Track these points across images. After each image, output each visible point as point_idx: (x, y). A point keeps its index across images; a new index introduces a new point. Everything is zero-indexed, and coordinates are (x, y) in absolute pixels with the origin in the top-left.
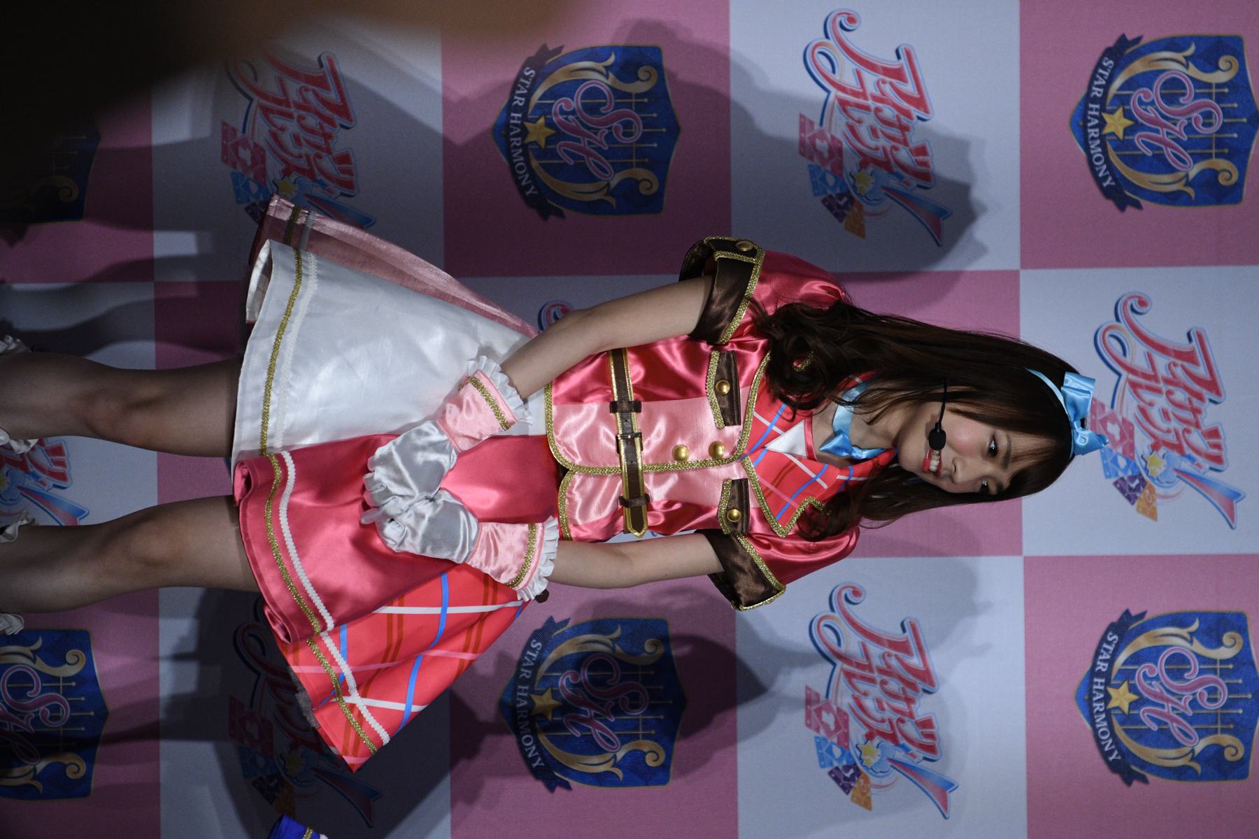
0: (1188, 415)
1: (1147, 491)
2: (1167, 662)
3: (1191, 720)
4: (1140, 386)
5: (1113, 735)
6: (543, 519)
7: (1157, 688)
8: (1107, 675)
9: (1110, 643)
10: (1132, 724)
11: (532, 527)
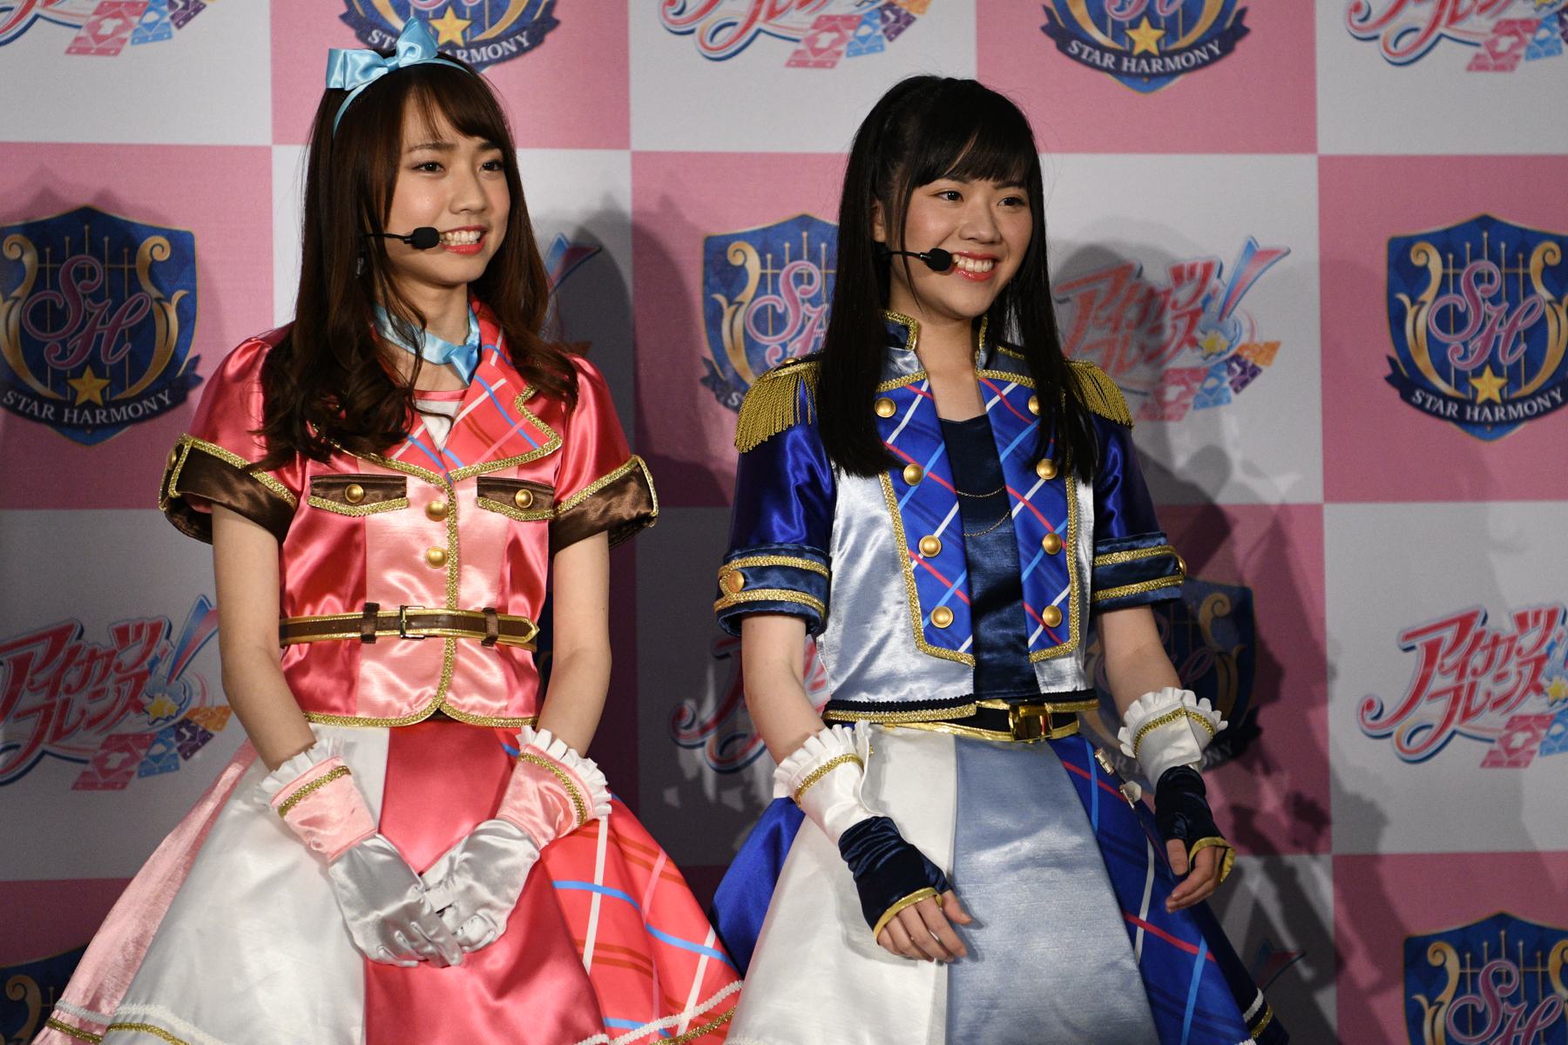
5: (498, 40)
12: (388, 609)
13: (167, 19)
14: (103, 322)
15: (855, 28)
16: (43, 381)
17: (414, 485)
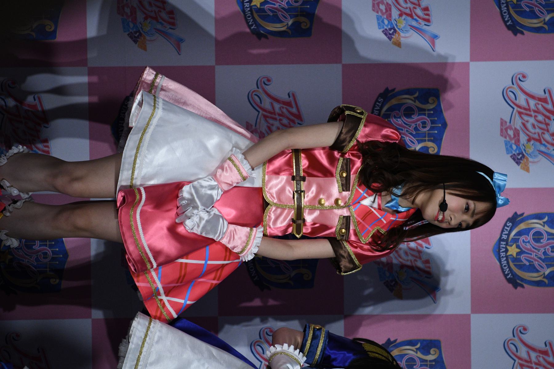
0: (544, 126)
1: (525, 160)
2: (533, 235)
3: (543, 261)
5: (509, 267)
6: (256, 226)
7: (528, 246)
8: (507, 241)
9: (508, 227)
10: (517, 262)
11: (251, 230)
13: (514, 152)
14: (407, 131)
16: (387, 111)
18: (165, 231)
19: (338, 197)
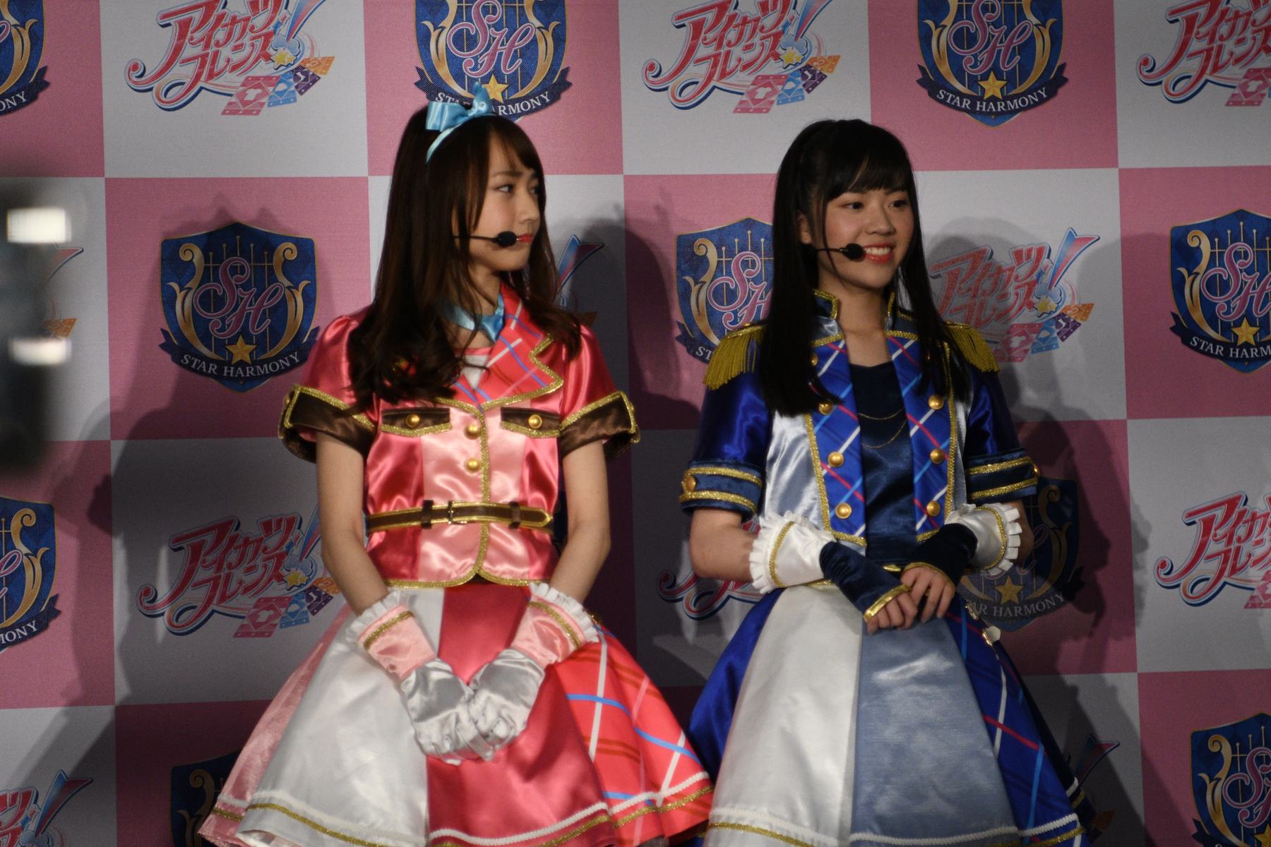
0: (238, 28)
4: (211, 71)
5: (527, 98)
7: (485, 59)
12: (440, 504)
13: (293, 88)
15: (783, 84)
16: (209, 346)
17: (456, 415)
18: (531, 787)
19: (461, 433)
